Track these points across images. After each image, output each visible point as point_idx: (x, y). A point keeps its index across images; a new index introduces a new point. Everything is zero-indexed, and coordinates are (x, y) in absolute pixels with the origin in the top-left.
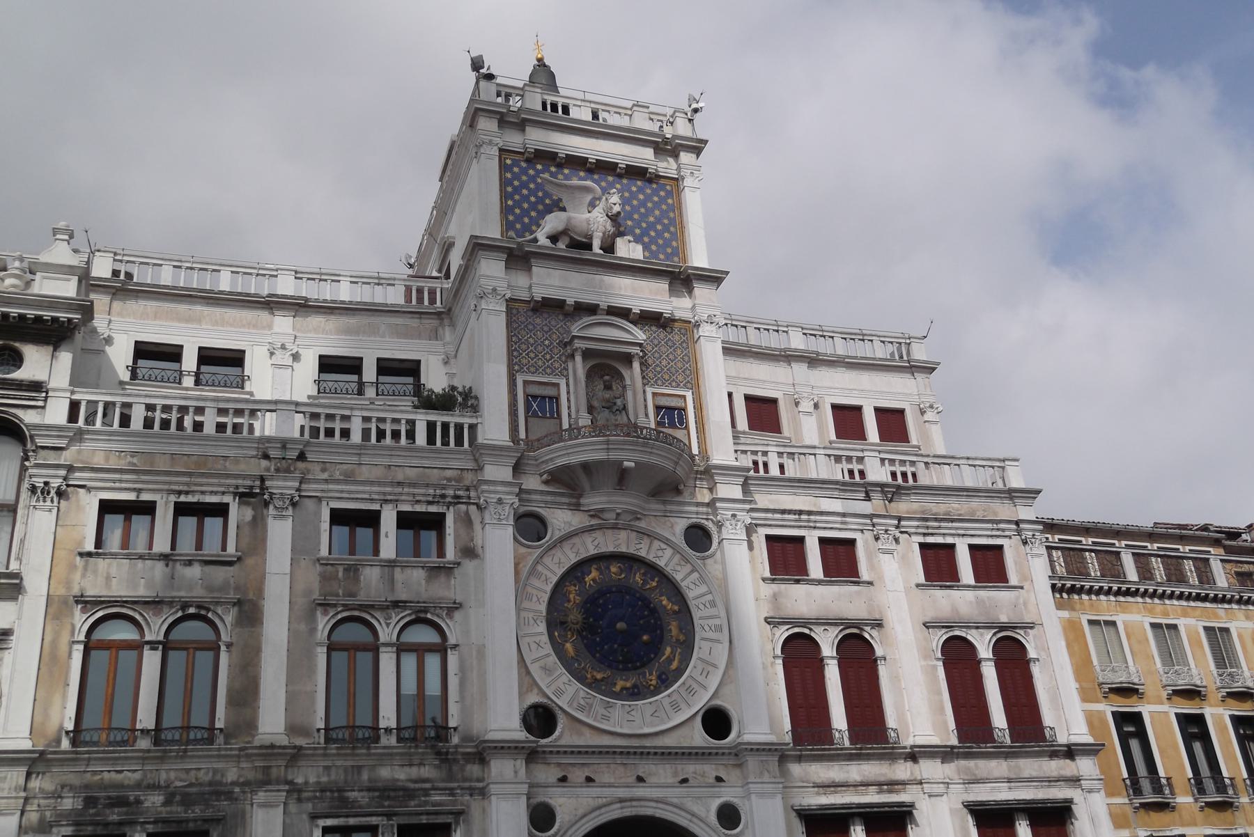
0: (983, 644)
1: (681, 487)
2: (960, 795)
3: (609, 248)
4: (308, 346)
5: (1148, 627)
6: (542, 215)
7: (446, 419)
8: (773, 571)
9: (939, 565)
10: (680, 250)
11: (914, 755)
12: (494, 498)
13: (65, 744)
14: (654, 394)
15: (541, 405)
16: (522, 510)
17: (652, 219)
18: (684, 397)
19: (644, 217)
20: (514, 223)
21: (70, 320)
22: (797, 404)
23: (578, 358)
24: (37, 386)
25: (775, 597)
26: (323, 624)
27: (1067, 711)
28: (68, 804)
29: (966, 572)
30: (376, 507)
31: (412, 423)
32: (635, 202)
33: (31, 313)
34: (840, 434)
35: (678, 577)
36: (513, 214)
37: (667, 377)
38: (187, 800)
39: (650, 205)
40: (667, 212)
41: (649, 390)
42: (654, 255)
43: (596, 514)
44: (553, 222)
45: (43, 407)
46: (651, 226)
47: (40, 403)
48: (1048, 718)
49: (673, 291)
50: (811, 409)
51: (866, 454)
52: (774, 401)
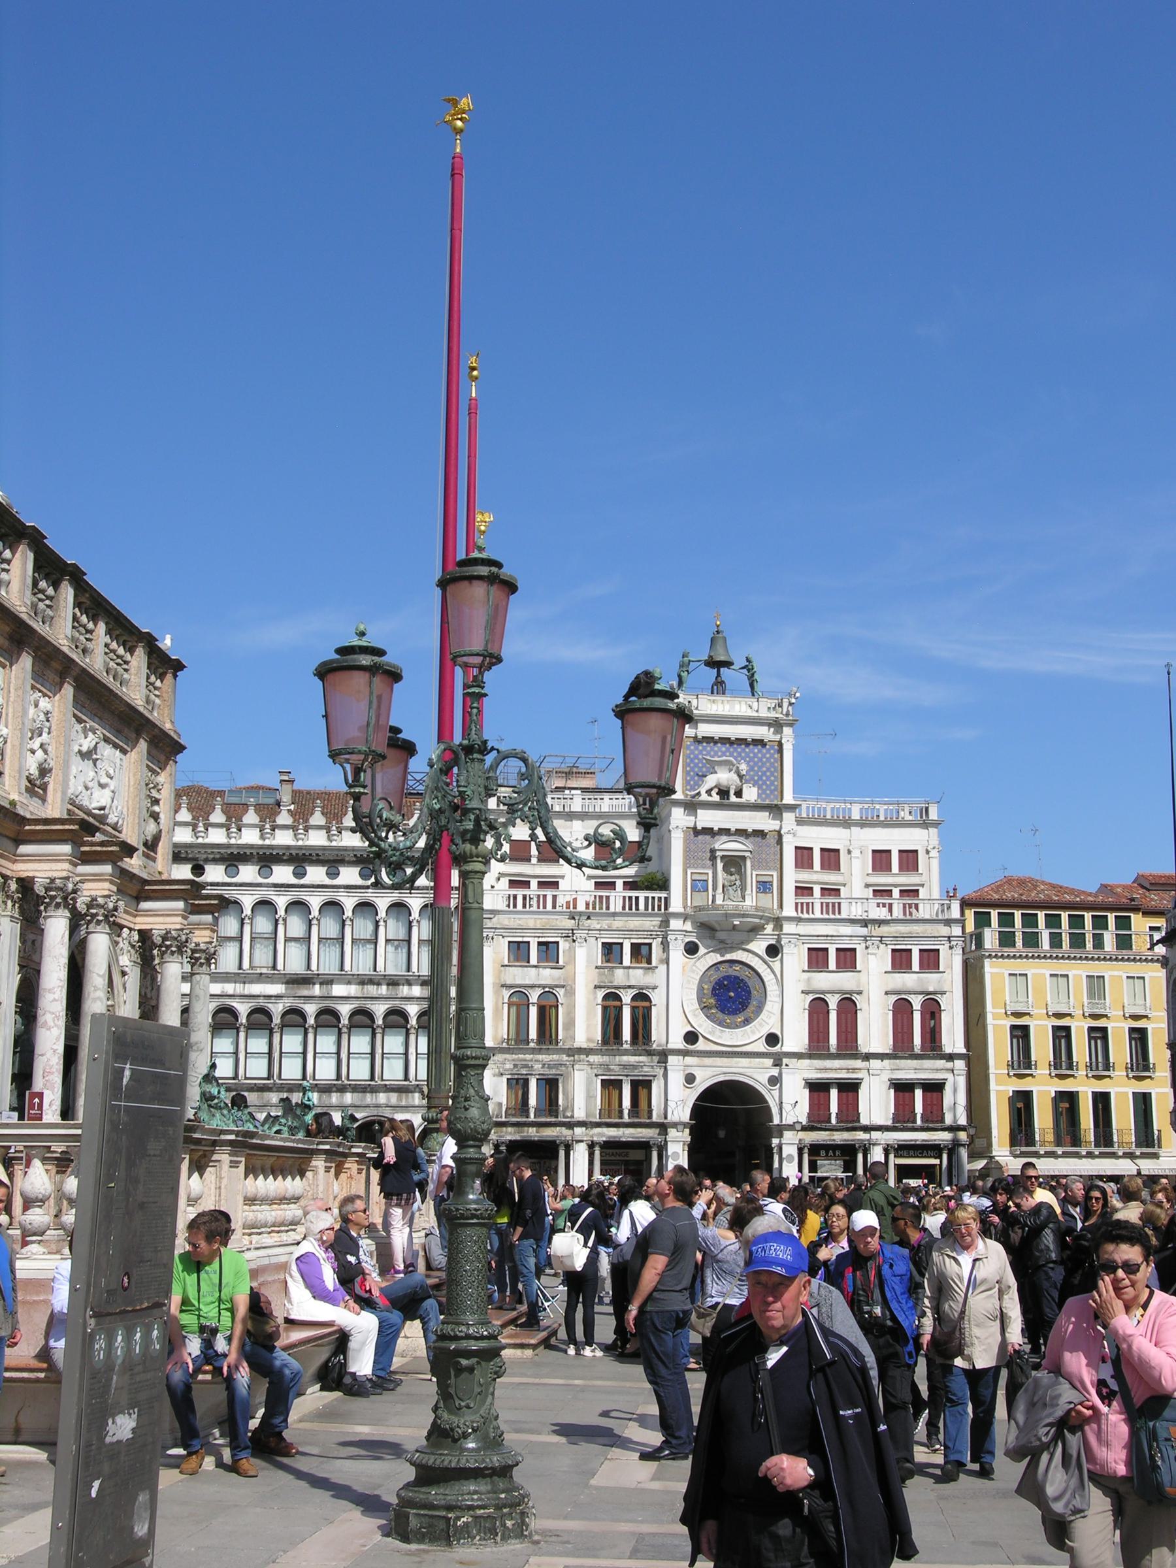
0: (917, 1002)
2: (886, 1076)
3: (739, 794)
5: (1048, 976)
8: (809, 966)
9: (901, 960)
11: (867, 1057)
12: (673, 937)
13: (505, 1045)
16: (687, 940)
23: (719, 861)
25: (809, 979)
26: (600, 994)
27: (953, 1038)
28: (507, 1066)
29: (916, 965)
30: (620, 941)
31: (637, 898)
34: (874, 869)
35: (760, 971)
38: (550, 1067)
41: (754, 873)
42: (764, 792)
43: (722, 942)
44: (711, 781)
46: (764, 773)
48: (945, 1040)
50: (858, 854)
52: (838, 851)
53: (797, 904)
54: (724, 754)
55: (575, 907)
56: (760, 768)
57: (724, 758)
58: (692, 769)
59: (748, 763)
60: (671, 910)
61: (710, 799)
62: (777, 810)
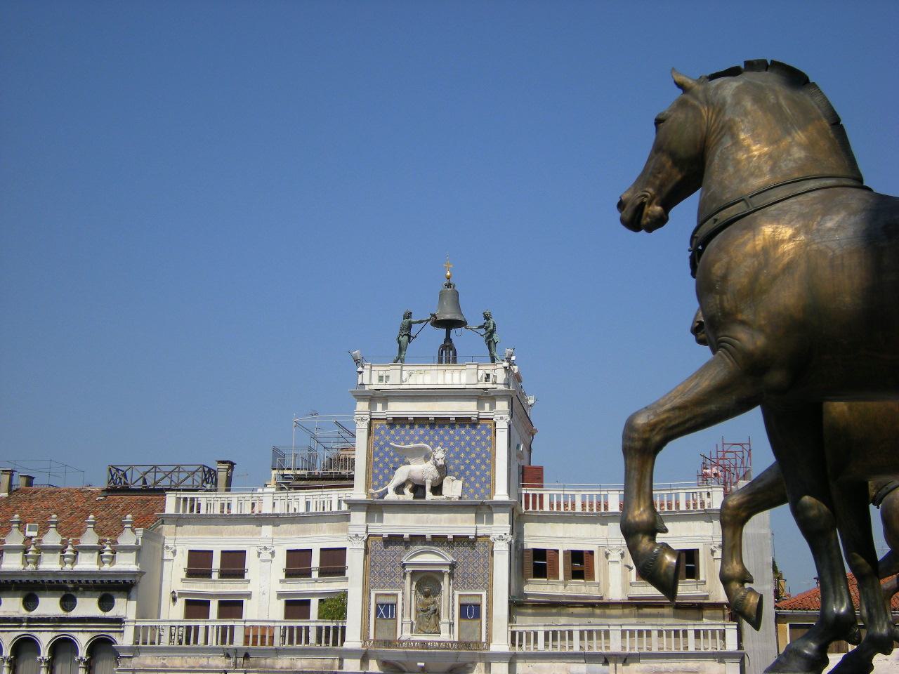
1: (470, 665)
3: (437, 489)
4: (279, 545)
6: (395, 469)
7: (328, 624)
10: (491, 482)
14: (460, 595)
15: (386, 611)
17: (473, 455)
18: (481, 595)
19: (468, 454)
20: (378, 474)
21: (131, 581)
22: (607, 555)
23: (408, 579)
24: (119, 621)
32: (463, 444)
33: (113, 580)
36: (378, 467)
37: (470, 581)
39: (473, 443)
40: (485, 447)
41: (457, 593)
42: (472, 485)
44: (400, 475)
45: (123, 631)
47: (122, 629)
49: (478, 519)
50: (618, 558)
51: (611, 628)
53: (513, 634)
54: (422, 439)
55: (231, 642)
56: (469, 453)
57: (422, 444)
58: (381, 460)
59: (452, 449)
60: (347, 645)
61: (401, 498)
62: (483, 509)
